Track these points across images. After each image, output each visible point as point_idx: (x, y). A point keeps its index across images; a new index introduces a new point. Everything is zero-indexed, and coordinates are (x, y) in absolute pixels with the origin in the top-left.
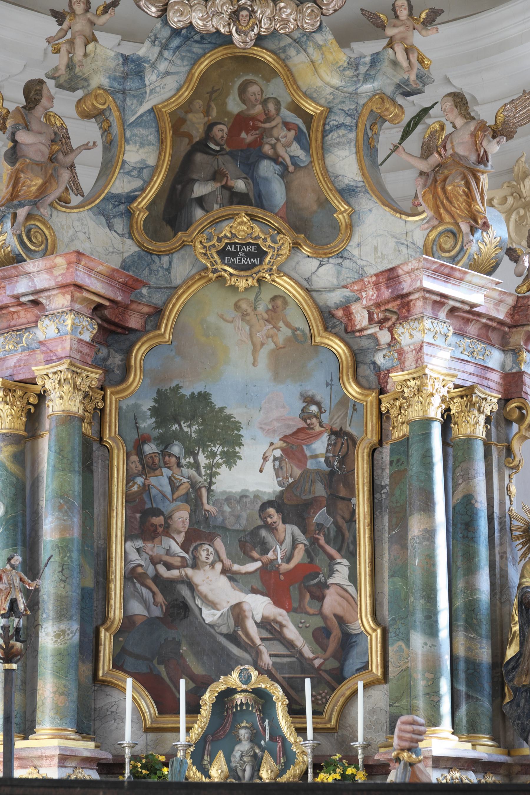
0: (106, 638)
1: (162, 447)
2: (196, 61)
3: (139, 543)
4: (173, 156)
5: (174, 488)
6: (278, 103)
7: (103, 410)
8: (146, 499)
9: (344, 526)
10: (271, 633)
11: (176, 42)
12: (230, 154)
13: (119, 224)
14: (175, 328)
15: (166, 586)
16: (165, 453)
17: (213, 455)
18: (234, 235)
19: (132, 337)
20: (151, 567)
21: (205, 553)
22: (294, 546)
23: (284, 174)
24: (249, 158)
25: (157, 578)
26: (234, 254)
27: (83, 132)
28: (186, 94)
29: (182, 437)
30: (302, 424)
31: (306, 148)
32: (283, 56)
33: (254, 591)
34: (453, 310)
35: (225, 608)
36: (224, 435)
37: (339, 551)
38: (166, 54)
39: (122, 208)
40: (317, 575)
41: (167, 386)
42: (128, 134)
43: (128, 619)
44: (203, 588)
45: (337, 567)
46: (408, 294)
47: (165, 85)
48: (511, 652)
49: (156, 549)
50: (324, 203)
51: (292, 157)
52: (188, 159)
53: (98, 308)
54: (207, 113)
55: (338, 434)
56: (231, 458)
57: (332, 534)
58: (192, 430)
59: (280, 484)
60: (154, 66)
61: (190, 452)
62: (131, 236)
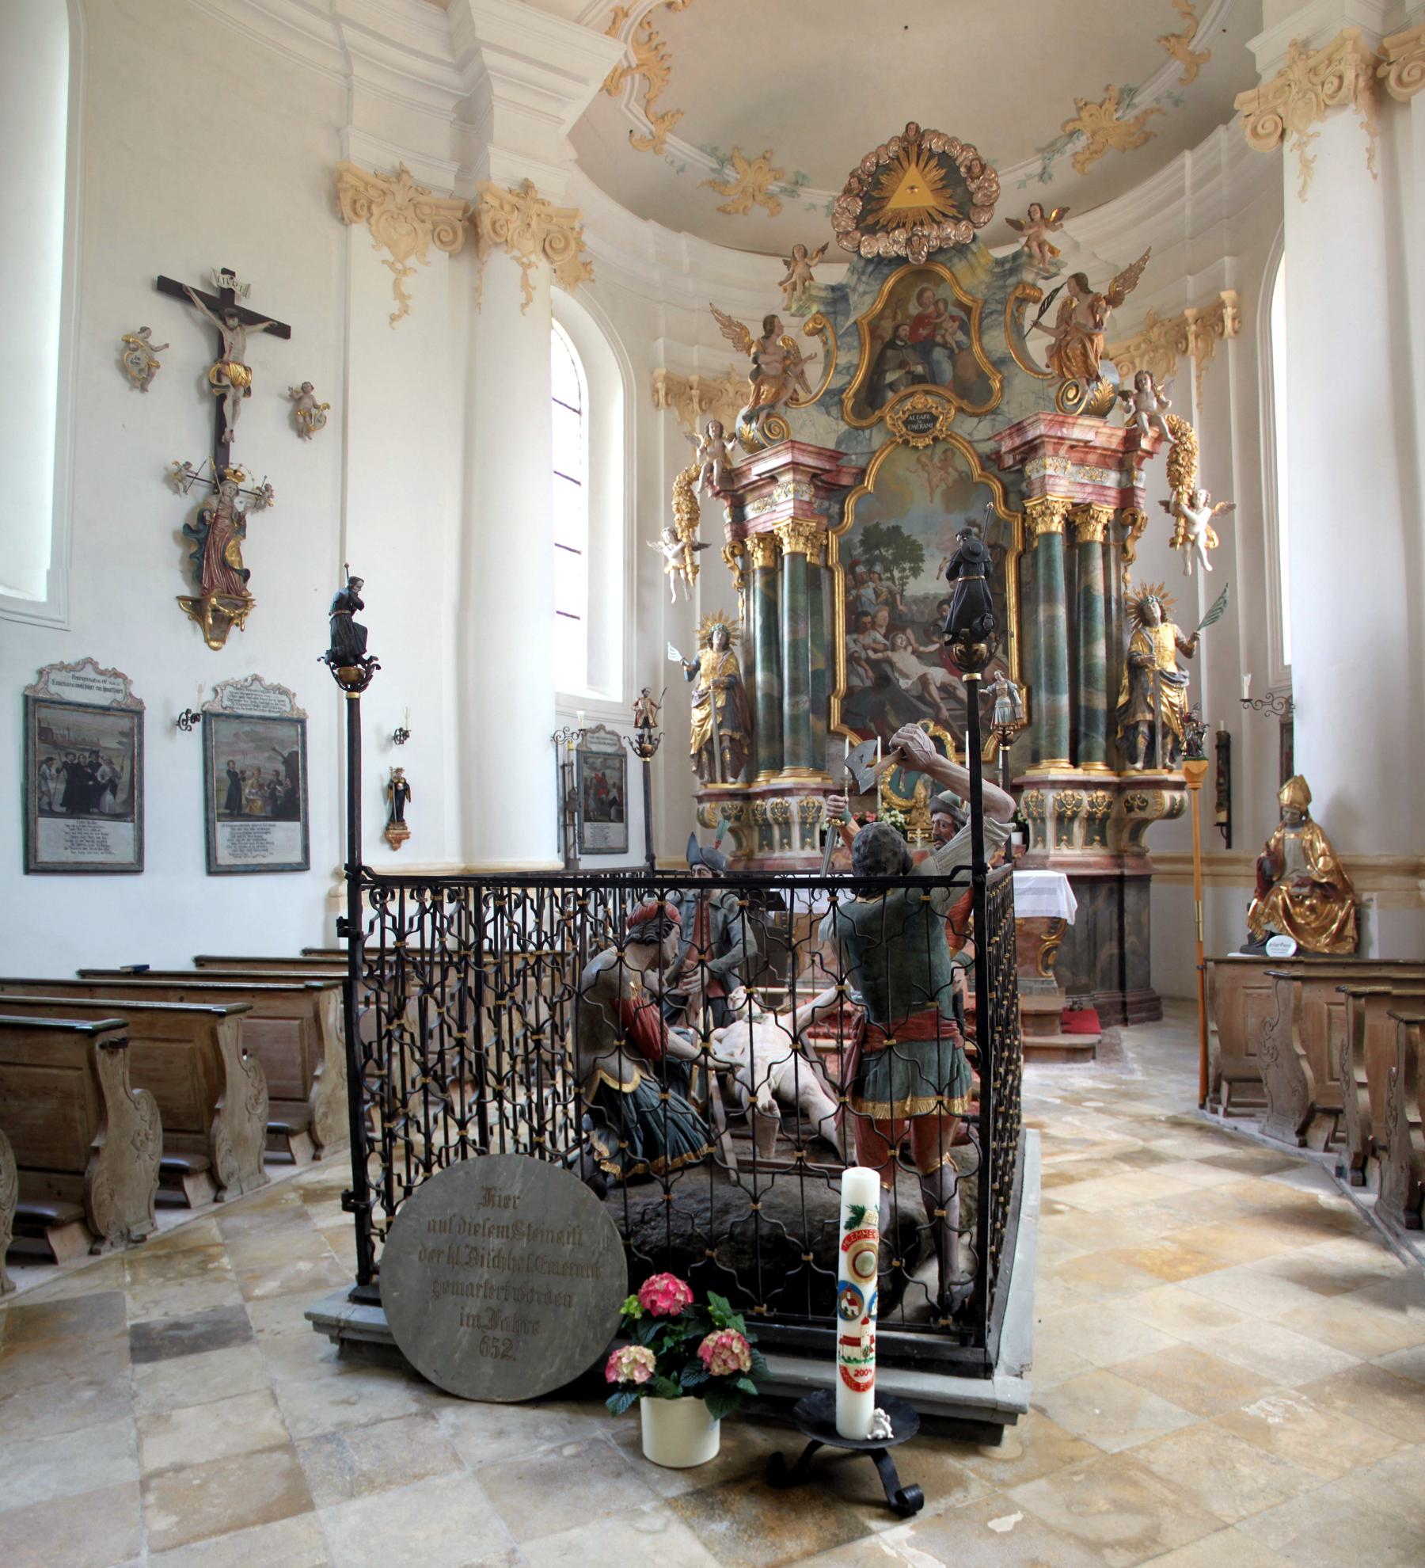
0: (835, 704)
2: (885, 280)
3: (855, 636)
5: (877, 595)
6: (946, 302)
11: (870, 268)
13: (834, 411)
15: (874, 664)
16: (870, 572)
17: (904, 570)
21: (900, 640)
23: (952, 356)
24: (924, 348)
25: (868, 660)
26: (915, 422)
27: (811, 346)
28: (880, 306)
29: (882, 559)
31: (967, 333)
33: (935, 665)
34: (1072, 447)
35: (915, 678)
36: (911, 554)
38: (864, 278)
39: (836, 399)
44: (900, 665)
47: (865, 304)
48: (1122, 699)
49: (866, 639)
50: (982, 376)
53: (814, 476)
54: (895, 318)
56: (916, 571)
58: (888, 553)
60: (854, 290)
61: (887, 569)
62: (843, 419)
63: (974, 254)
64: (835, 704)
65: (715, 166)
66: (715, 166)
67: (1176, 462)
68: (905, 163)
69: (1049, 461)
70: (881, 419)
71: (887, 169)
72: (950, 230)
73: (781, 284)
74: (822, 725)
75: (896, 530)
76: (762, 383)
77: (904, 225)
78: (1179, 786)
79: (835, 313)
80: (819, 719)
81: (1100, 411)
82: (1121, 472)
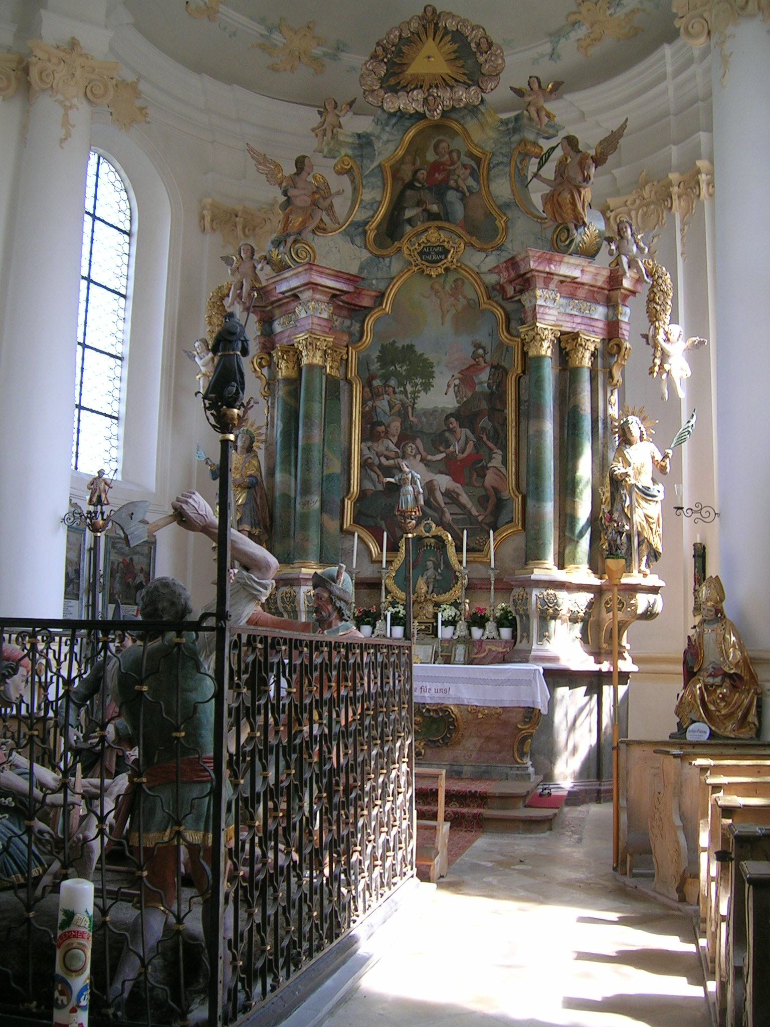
0: (348, 504)
1: (383, 382)
3: (369, 444)
4: (392, 194)
5: (391, 407)
6: (459, 153)
7: (347, 359)
8: (374, 415)
9: (499, 428)
10: (450, 499)
11: (394, 121)
12: (428, 188)
13: (358, 240)
14: (393, 305)
16: (385, 385)
18: (428, 241)
19: (366, 312)
20: (377, 459)
21: (410, 449)
22: (466, 444)
23: (463, 198)
24: (440, 191)
25: (380, 466)
26: (429, 254)
28: (401, 153)
29: (396, 374)
30: (473, 362)
31: (477, 180)
32: (462, 122)
33: (441, 473)
36: (424, 372)
37: (496, 445)
38: (388, 129)
39: (360, 229)
40: (481, 461)
41: (386, 342)
42: (364, 182)
43: (363, 493)
45: (494, 455)
46: (526, 273)
47: (389, 148)
49: (380, 447)
50: (489, 215)
51: (468, 187)
52: (402, 193)
53: (334, 296)
54: (414, 164)
55: (496, 367)
56: (427, 387)
57: (491, 434)
58: (402, 369)
59: (458, 402)
60: (378, 138)
62: (366, 247)
63: (483, 114)
64: (348, 504)
65: (265, 32)
66: (265, 32)
67: (653, 300)
68: (423, 37)
69: (539, 292)
70: (399, 250)
71: (409, 41)
72: (461, 93)
73: (313, 130)
74: (336, 524)
75: (411, 348)
76: (291, 212)
77: (421, 87)
78: (654, 590)
79: (362, 156)
80: (333, 519)
81: (590, 253)
82: (608, 307)
